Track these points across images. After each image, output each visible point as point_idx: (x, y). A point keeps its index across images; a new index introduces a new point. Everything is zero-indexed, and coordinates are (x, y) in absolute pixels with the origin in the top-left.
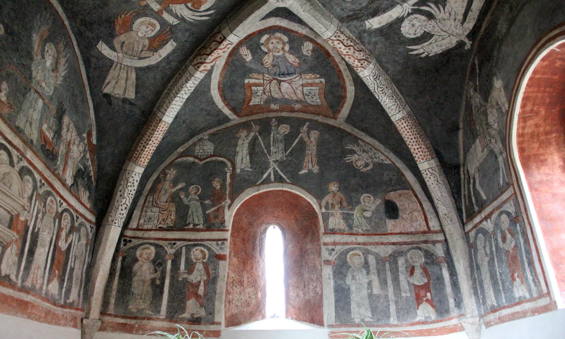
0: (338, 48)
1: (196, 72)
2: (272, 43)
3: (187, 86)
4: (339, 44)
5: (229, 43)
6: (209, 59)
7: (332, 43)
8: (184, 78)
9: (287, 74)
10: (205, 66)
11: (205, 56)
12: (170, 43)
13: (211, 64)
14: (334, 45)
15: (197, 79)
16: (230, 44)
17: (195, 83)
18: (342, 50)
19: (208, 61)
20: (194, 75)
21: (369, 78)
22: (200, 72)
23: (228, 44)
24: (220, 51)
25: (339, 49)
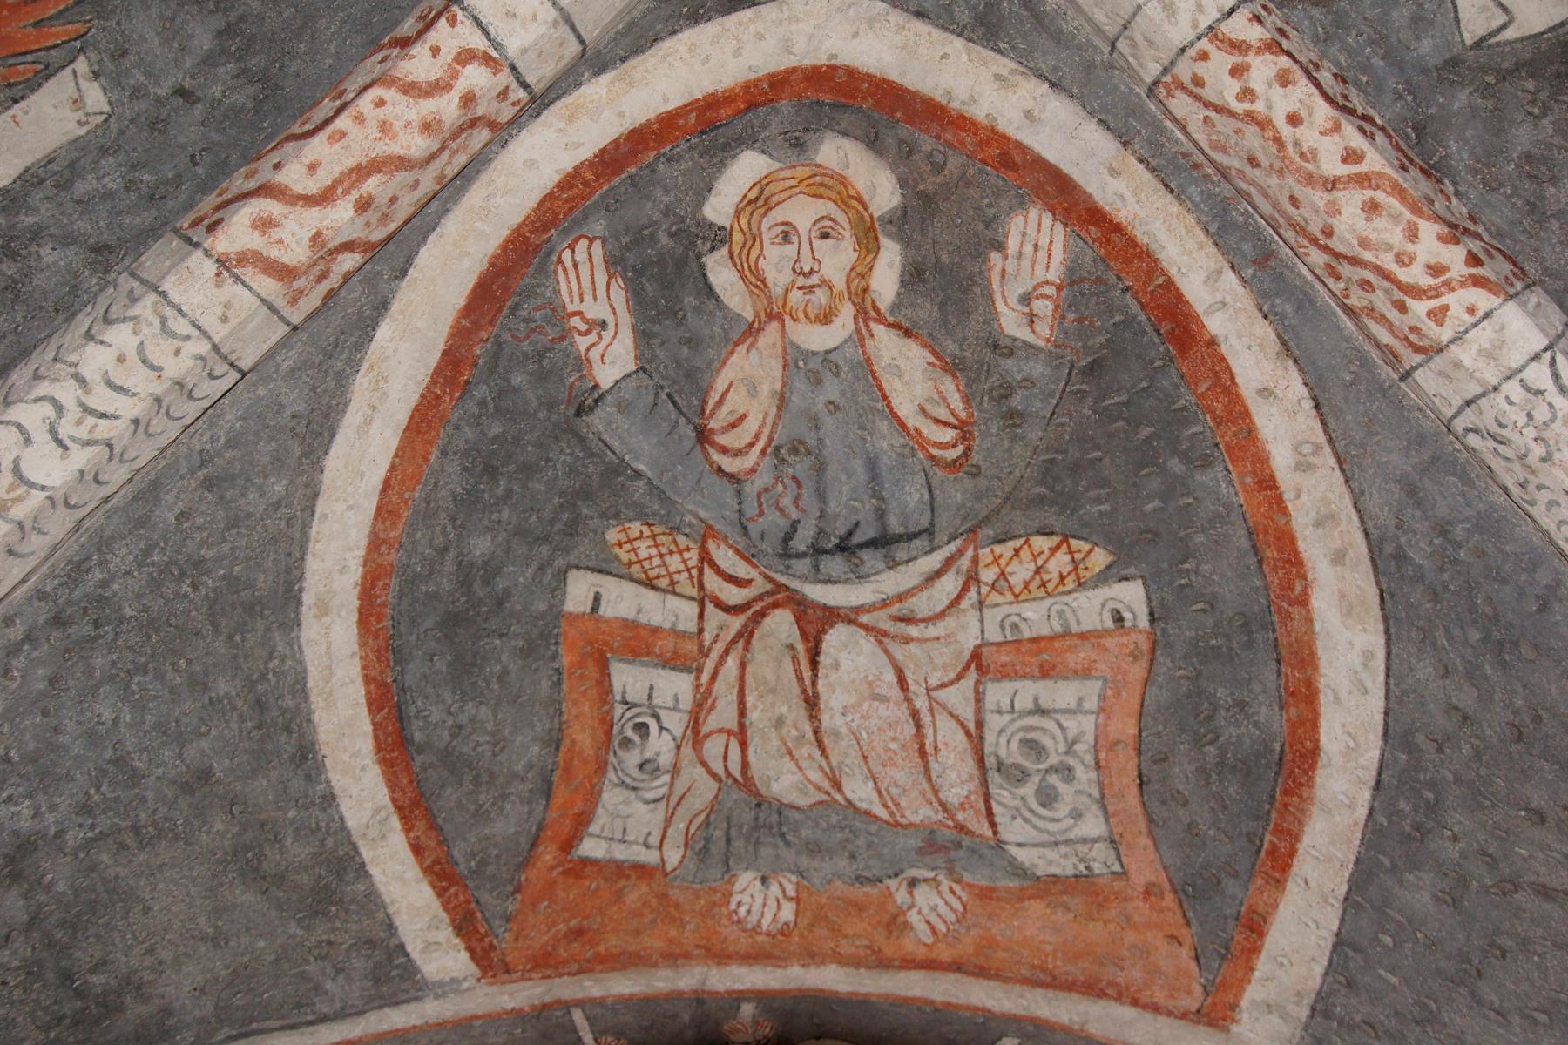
0: (1280, 120)
1: (189, 254)
2: (787, 234)
3: (86, 372)
4: (1284, 80)
5: (478, 42)
6: (313, 167)
7: (1237, 71)
8: (82, 322)
9: (872, 544)
10: (264, 225)
11: (274, 158)
12: (58, 89)
13: (314, 218)
14: (1247, 94)
15: (182, 327)
16: (487, 60)
17: (154, 357)
18: (1309, 136)
19: (294, 176)
20: (166, 286)
21: (1547, 384)
22: (222, 262)
23: (466, 57)
24: (405, 110)
25: (1286, 131)
